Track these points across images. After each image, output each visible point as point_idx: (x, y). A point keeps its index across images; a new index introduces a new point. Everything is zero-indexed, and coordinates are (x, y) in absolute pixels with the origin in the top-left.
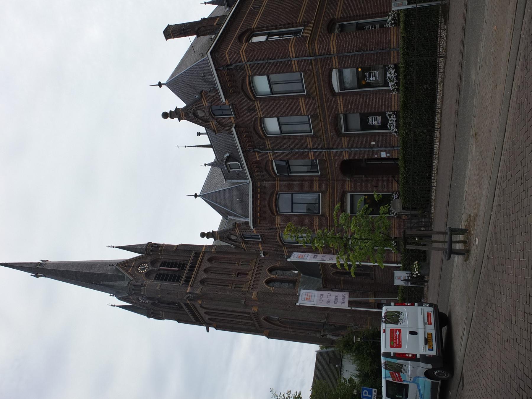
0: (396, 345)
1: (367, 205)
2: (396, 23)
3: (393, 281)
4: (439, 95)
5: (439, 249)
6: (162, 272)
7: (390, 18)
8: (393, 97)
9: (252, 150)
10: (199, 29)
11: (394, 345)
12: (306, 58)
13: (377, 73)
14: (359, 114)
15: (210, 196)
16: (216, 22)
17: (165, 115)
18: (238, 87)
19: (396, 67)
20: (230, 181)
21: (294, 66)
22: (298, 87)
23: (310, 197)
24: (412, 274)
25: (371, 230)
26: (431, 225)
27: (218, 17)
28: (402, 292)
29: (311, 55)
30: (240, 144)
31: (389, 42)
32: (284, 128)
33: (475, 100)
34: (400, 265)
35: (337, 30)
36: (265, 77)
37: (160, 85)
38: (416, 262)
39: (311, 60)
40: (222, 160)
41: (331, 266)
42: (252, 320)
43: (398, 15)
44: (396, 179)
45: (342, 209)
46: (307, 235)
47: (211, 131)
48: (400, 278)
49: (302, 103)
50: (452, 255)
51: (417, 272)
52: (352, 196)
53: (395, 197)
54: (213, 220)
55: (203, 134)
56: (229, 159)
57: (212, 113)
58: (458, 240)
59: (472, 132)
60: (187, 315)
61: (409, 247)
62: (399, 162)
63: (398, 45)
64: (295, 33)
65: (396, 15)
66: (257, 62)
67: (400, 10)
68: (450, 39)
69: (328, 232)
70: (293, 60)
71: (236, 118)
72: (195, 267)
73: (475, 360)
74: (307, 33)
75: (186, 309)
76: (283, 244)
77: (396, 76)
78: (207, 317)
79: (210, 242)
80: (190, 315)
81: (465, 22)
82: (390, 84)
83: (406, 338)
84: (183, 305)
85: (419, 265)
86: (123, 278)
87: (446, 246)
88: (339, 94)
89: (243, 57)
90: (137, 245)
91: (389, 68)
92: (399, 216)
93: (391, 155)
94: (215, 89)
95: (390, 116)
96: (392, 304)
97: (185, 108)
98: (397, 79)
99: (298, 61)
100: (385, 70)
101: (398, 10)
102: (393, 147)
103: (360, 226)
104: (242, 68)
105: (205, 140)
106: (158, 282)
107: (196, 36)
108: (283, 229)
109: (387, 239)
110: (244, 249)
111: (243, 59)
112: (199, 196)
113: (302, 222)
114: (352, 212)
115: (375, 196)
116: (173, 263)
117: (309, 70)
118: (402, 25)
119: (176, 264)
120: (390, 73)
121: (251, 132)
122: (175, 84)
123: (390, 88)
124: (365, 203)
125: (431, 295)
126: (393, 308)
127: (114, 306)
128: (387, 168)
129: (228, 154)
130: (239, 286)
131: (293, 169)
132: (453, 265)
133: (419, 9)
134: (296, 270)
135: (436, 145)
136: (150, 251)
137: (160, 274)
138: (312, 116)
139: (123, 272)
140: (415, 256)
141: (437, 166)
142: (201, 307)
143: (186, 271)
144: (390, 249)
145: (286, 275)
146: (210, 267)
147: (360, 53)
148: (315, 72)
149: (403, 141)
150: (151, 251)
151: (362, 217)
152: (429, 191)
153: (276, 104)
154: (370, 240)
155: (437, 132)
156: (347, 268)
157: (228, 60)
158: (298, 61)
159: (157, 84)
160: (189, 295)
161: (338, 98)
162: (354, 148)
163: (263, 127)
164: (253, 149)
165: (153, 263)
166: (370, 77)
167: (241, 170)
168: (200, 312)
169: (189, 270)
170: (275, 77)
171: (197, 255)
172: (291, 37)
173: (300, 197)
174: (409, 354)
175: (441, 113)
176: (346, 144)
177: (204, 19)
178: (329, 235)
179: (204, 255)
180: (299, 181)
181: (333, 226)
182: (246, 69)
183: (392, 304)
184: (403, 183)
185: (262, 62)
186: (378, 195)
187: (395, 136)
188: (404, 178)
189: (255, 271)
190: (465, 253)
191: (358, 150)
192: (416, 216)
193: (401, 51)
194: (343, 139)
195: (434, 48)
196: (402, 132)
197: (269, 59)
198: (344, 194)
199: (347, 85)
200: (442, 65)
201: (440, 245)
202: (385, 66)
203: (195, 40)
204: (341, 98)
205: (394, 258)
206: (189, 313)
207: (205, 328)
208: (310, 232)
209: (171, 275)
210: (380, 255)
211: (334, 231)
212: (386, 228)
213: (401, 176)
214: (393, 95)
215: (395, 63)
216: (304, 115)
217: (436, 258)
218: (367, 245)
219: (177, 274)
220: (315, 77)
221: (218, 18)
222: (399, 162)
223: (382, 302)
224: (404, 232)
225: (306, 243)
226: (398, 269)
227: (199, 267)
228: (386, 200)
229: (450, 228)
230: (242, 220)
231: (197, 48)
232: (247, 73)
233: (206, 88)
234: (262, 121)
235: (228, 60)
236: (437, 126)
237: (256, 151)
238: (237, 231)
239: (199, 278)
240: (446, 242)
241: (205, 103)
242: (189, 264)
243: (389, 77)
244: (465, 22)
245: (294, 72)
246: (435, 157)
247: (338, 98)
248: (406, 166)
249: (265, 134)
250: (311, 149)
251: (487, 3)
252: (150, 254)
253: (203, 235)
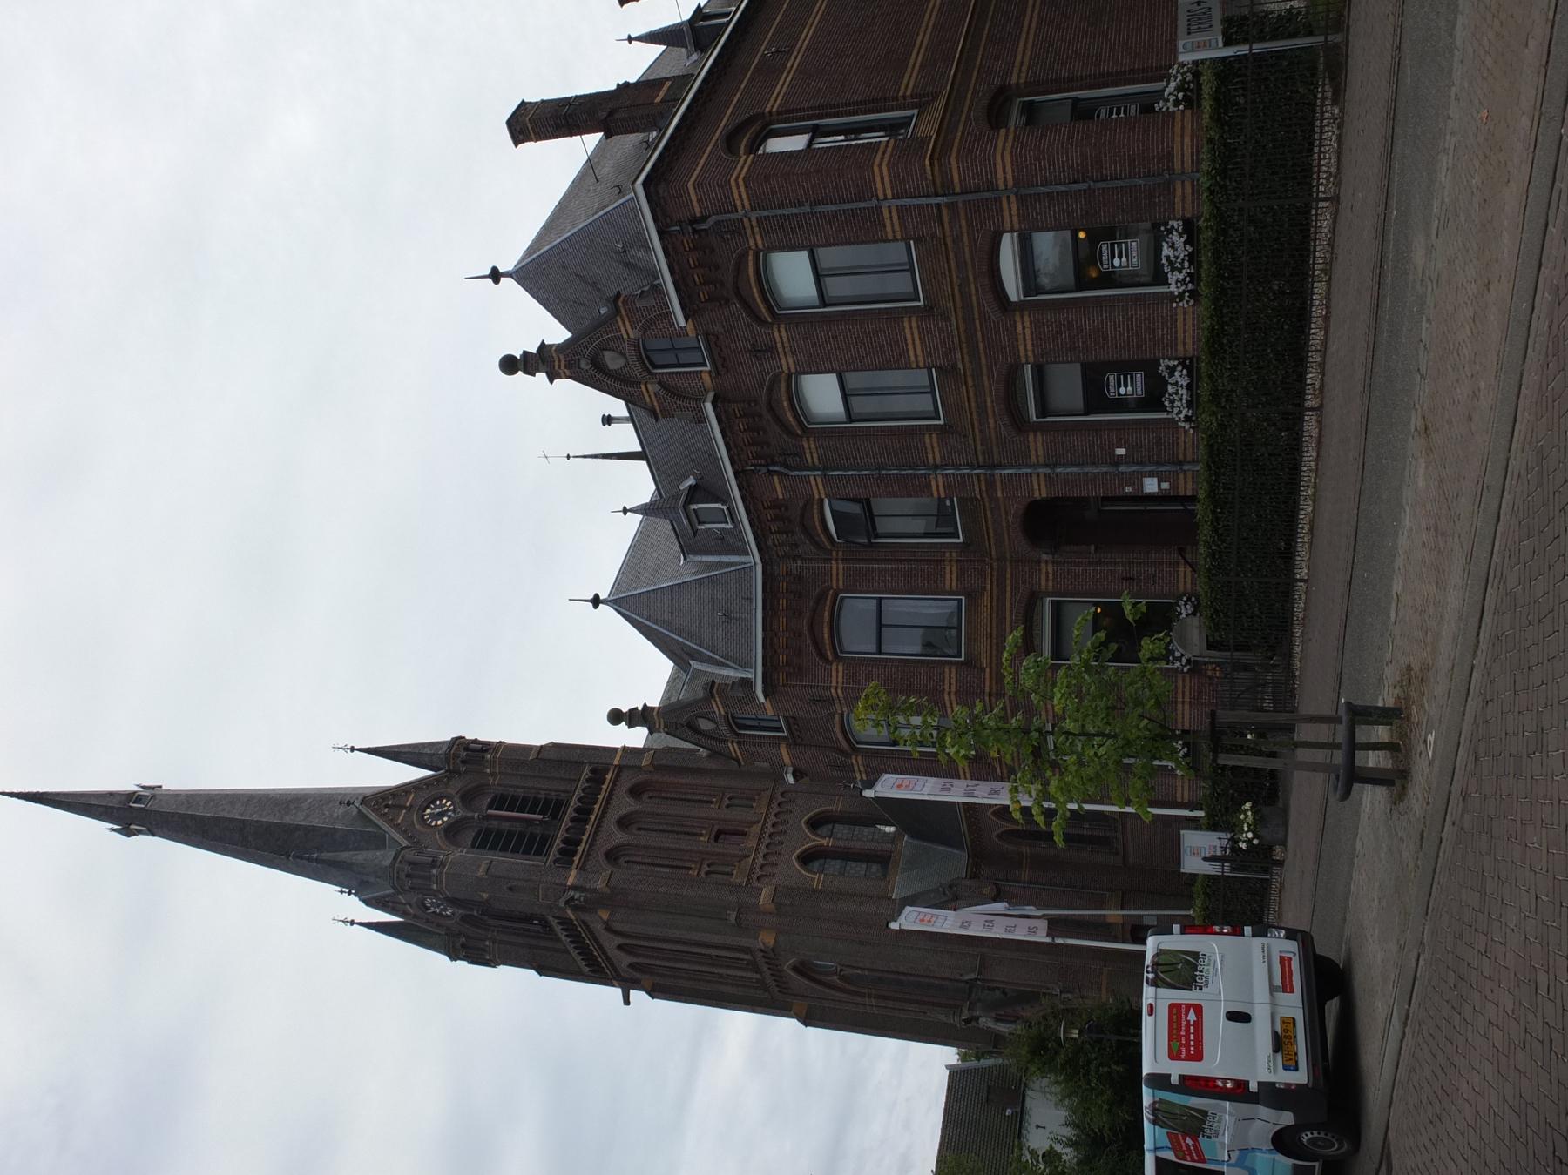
0: (1188, 1050)
1: (1102, 635)
2: (1191, 97)
3: (1178, 861)
4: (1317, 312)
5: (1314, 767)
6: (495, 824)
7: (1173, 85)
8: (1180, 317)
9: (764, 470)
10: (611, 113)
11: (1180, 1052)
12: (923, 201)
13: (1134, 245)
14: (1078, 366)
15: (637, 602)
16: (662, 94)
17: (510, 365)
18: (722, 284)
19: (1190, 229)
20: (698, 558)
21: (888, 223)
22: (899, 284)
23: (931, 609)
24: (1234, 841)
25: (1114, 708)
26: (1293, 696)
27: (667, 79)
28: (1205, 893)
29: (940, 191)
30: (728, 449)
31: (1170, 155)
32: (859, 405)
33: (1425, 324)
34: (1201, 814)
35: (1015, 119)
36: (804, 255)
37: (495, 275)
38: (1248, 805)
39: (938, 206)
40: (676, 497)
41: (994, 813)
42: (758, 971)
43: (1197, 75)
44: (1188, 557)
45: (1029, 645)
46: (924, 722)
47: (642, 413)
48: (1200, 851)
49: (911, 329)
50: (1356, 786)
51: (1250, 835)
52: (1057, 607)
53: (1184, 610)
54: (647, 674)
55: (620, 420)
56: (694, 494)
57: (648, 361)
58: (1373, 740)
59: (1416, 421)
60: (567, 952)
61: (1226, 760)
62: (1198, 508)
63: (1196, 163)
64: (892, 128)
65: (1189, 77)
66: (779, 212)
67: (1203, 61)
68: (1350, 150)
69: (984, 712)
70: (885, 204)
71: (716, 373)
72: (590, 811)
73: (1425, 1101)
74: (928, 128)
75: (562, 935)
76: (853, 745)
77: (1190, 255)
78: (624, 960)
79: (637, 737)
80: (574, 953)
81: (1395, 98)
82: (1173, 278)
83: (1217, 1031)
84: (554, 922)
85: (1254, 814)
86: (378, 841)
87: (1339, 757)
88: (1021, 306)
89: (740, 195)
90: (423, 745)
91: (1170, 232)
92: (1196, 667)
93: (1174, 486)
94: (658, 290)
95: (1172, 371)
96: (1176, 928)
97: (568, 343)
98: (1191, 263)
99: (900, 209)
100: (1157, 237)
101: (1195, 63)
102: (1181, 463)
103: (1079, 695)
104: (738, 229)
105: (625, 436)
106: (482, 855)
107: (600, 135)
108: (851, 701)
109: (1162, 736)
110: (737, 760)
111: (738, 203)
112: (606, 602)
113: (909, 682)
114: (1057, 653)
115: (1127, 609)
116: (525, 799)
117: (933, 236)
118: (1207, 105)
119: (536, 801)
120: (1172, 246)
121: (760, 416)
122: (541, 274)
123: (1173, 288)
124: (1096, 629)
125: (1293, 904)
126: (1177, 941)
127: (352, 923)
128: (1159, 526)
129: (691, 481)
130: (721, 869)
131: (883, 526)
132: (1358, 813)
133: (1259, 58)
134: (891, 825)
135: (1309, 457)
136: (460, 762)
137: (488, 832)
138: (940, 369)
139: (380, 822)
140: (1245, 788)
141: (1312, 522)
142: (609, 929)
143: (566, 823)
144: (1171, 764)
145: (860, 838)
146: (632, 813)
147: (1084, 186)
148: (949, 240)
149: (1210, 446)
150: (463, 762)
151: (1088, 669)
152: (1287, 595)
153: (833, 334)
154: (1109, 736)
155: (1310, 420)
156: (1040, 819)
157: (695, 204)
158: (900, 209)
159: (488, 272)
160: (572, 893)
161: (1018, 319)
162: (1064, 465)
163: (796, 401)
164: (767, 465)
165: (467, 798)
166: (1113, 257)
167: (730, 526)
168: (606, 945)
169: (572, 820)
170: (831, 256)
171: (598, 776)
172: (879, 138)
173: (903, 607)
174: (1225, 1080)
175: (1322, 365)
176: (1040, 453)
177: (627, 84)
178: (990, 720)
179: (618, 775)
180: (900, 561)
181: (1000, 694)
182: (748, 231)
183: (1176, 928)
184: (1209, 570)
185: (795, 211)
186: (1134, 605)
187: (1186, 432)
188: (1213, 553)
189: (769, 825)
190: (1395, 780)
191: (1075, 470)
192: (1246, 668)
193: (1205, 182)
194: (1031, 437)
195: (1303, 174)
196: (1205, 417)
197: (817, 203)
198: (1033, 599)
199: (1045, 281)
200: (1325, 223)
201: (1320, 756)
202: (1155, 226)
203: (599, 148)
204: (1026, 319)
205: (1183, 793)
206: (571, 947)
207: (618, 991)
208: (932, 714)
209: (522, 835)
210: (1139, 784)
211: (1004, 709)
212: (1158, 704)
213: (1202, 550)
214: (1180, 311)
215: (1188, 215)
216: (918, 367)
217: (1306, 792)
218: (1102, 751)
219: (539, 831)
220: (952, 255)
221: (668, 84)
222: (1198, 508)
223: (1146, 922)
224: (1213, 714)
225: (921, 744)
226: (1193, 824)
227: (605, 812)
228: (1159, 619)
229: (1348, 704)
230: (731, 673)
231: (606, 170)
232: (752, 242)
233: (630, 285)
234: (792, 382)
235: (695, 204)
236: (1311, 402)
238: (718, 707)
239: (603, 846)
240: (1334, 746)
241: (628, 331)
242: (574, 803)
243: (1168, 258)
244: (1395, 98)
245: (887, 241)
246: (1306, 492)
247: (1018, 319)
248: (1217, 519)
249: (801, 423)
250: (936, 467)
251: (1458, 42)
252: (458, 773)
253: (616, 717)
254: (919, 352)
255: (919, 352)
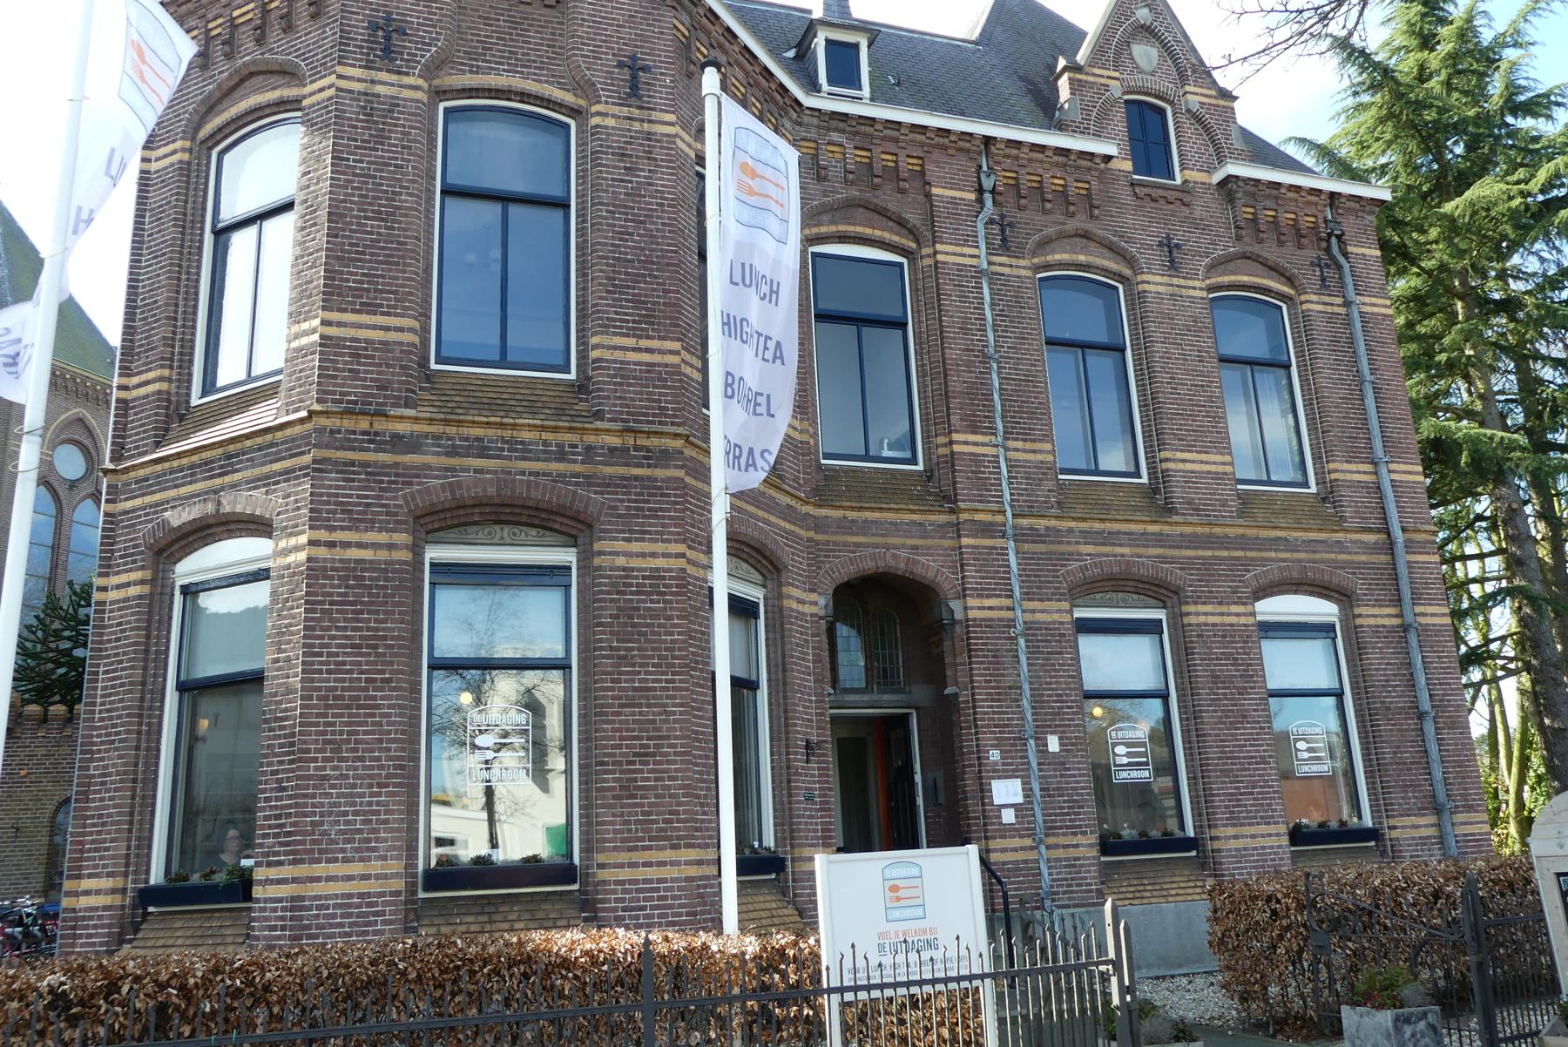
21: (1353, 467)
111: (1367, 300)
197: (1377, 390)
237: (980, 201)
254: (1189, 466)
255: (1189, 466)
